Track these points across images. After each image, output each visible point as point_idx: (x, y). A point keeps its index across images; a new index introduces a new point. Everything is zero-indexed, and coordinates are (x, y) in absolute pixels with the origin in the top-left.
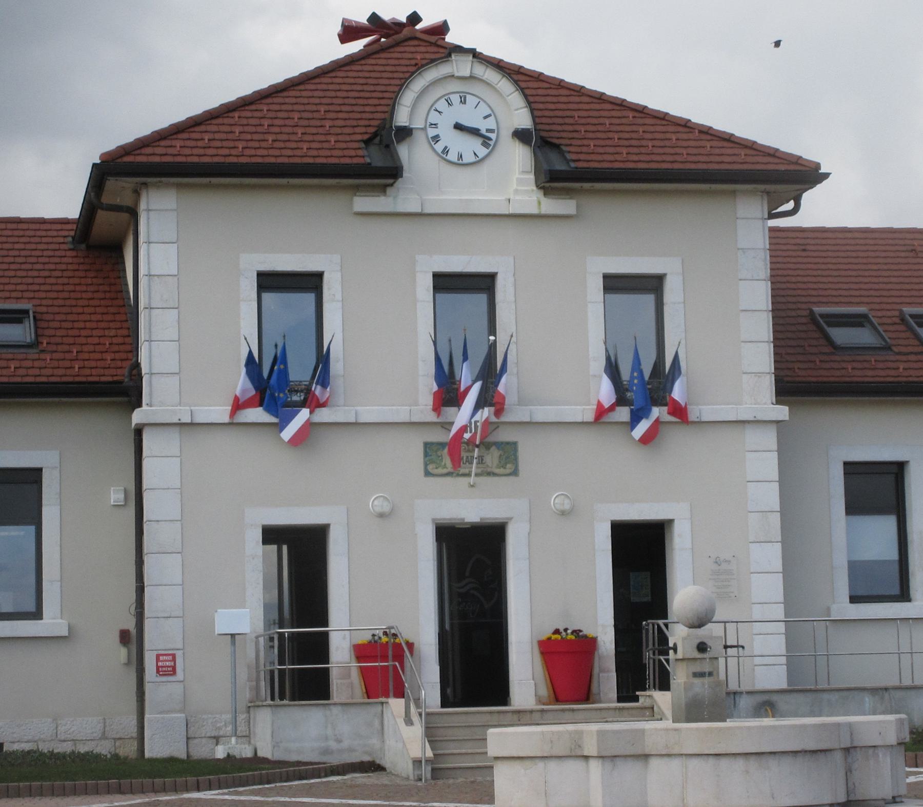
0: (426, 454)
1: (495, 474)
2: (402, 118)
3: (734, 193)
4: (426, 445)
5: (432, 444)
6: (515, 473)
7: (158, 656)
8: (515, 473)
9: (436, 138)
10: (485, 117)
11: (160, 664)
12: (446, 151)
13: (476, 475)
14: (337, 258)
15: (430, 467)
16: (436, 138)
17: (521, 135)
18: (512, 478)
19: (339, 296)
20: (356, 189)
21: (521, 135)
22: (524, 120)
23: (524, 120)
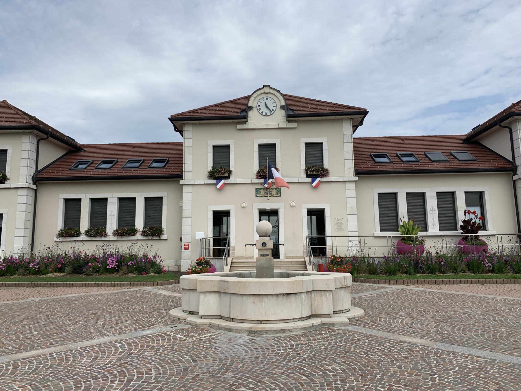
0: (256, 191)
2: (250, 104)
3: (342, 119)
4: (256, 189)
6: (280, 196)
8: (280, 196)
9: (260, 109)
14: (233, 141)
16: (260, 109)
17: (282, 107)
20: (239, 123)
21: (282, 107)
22: (283, 103)
23: (283, 103)
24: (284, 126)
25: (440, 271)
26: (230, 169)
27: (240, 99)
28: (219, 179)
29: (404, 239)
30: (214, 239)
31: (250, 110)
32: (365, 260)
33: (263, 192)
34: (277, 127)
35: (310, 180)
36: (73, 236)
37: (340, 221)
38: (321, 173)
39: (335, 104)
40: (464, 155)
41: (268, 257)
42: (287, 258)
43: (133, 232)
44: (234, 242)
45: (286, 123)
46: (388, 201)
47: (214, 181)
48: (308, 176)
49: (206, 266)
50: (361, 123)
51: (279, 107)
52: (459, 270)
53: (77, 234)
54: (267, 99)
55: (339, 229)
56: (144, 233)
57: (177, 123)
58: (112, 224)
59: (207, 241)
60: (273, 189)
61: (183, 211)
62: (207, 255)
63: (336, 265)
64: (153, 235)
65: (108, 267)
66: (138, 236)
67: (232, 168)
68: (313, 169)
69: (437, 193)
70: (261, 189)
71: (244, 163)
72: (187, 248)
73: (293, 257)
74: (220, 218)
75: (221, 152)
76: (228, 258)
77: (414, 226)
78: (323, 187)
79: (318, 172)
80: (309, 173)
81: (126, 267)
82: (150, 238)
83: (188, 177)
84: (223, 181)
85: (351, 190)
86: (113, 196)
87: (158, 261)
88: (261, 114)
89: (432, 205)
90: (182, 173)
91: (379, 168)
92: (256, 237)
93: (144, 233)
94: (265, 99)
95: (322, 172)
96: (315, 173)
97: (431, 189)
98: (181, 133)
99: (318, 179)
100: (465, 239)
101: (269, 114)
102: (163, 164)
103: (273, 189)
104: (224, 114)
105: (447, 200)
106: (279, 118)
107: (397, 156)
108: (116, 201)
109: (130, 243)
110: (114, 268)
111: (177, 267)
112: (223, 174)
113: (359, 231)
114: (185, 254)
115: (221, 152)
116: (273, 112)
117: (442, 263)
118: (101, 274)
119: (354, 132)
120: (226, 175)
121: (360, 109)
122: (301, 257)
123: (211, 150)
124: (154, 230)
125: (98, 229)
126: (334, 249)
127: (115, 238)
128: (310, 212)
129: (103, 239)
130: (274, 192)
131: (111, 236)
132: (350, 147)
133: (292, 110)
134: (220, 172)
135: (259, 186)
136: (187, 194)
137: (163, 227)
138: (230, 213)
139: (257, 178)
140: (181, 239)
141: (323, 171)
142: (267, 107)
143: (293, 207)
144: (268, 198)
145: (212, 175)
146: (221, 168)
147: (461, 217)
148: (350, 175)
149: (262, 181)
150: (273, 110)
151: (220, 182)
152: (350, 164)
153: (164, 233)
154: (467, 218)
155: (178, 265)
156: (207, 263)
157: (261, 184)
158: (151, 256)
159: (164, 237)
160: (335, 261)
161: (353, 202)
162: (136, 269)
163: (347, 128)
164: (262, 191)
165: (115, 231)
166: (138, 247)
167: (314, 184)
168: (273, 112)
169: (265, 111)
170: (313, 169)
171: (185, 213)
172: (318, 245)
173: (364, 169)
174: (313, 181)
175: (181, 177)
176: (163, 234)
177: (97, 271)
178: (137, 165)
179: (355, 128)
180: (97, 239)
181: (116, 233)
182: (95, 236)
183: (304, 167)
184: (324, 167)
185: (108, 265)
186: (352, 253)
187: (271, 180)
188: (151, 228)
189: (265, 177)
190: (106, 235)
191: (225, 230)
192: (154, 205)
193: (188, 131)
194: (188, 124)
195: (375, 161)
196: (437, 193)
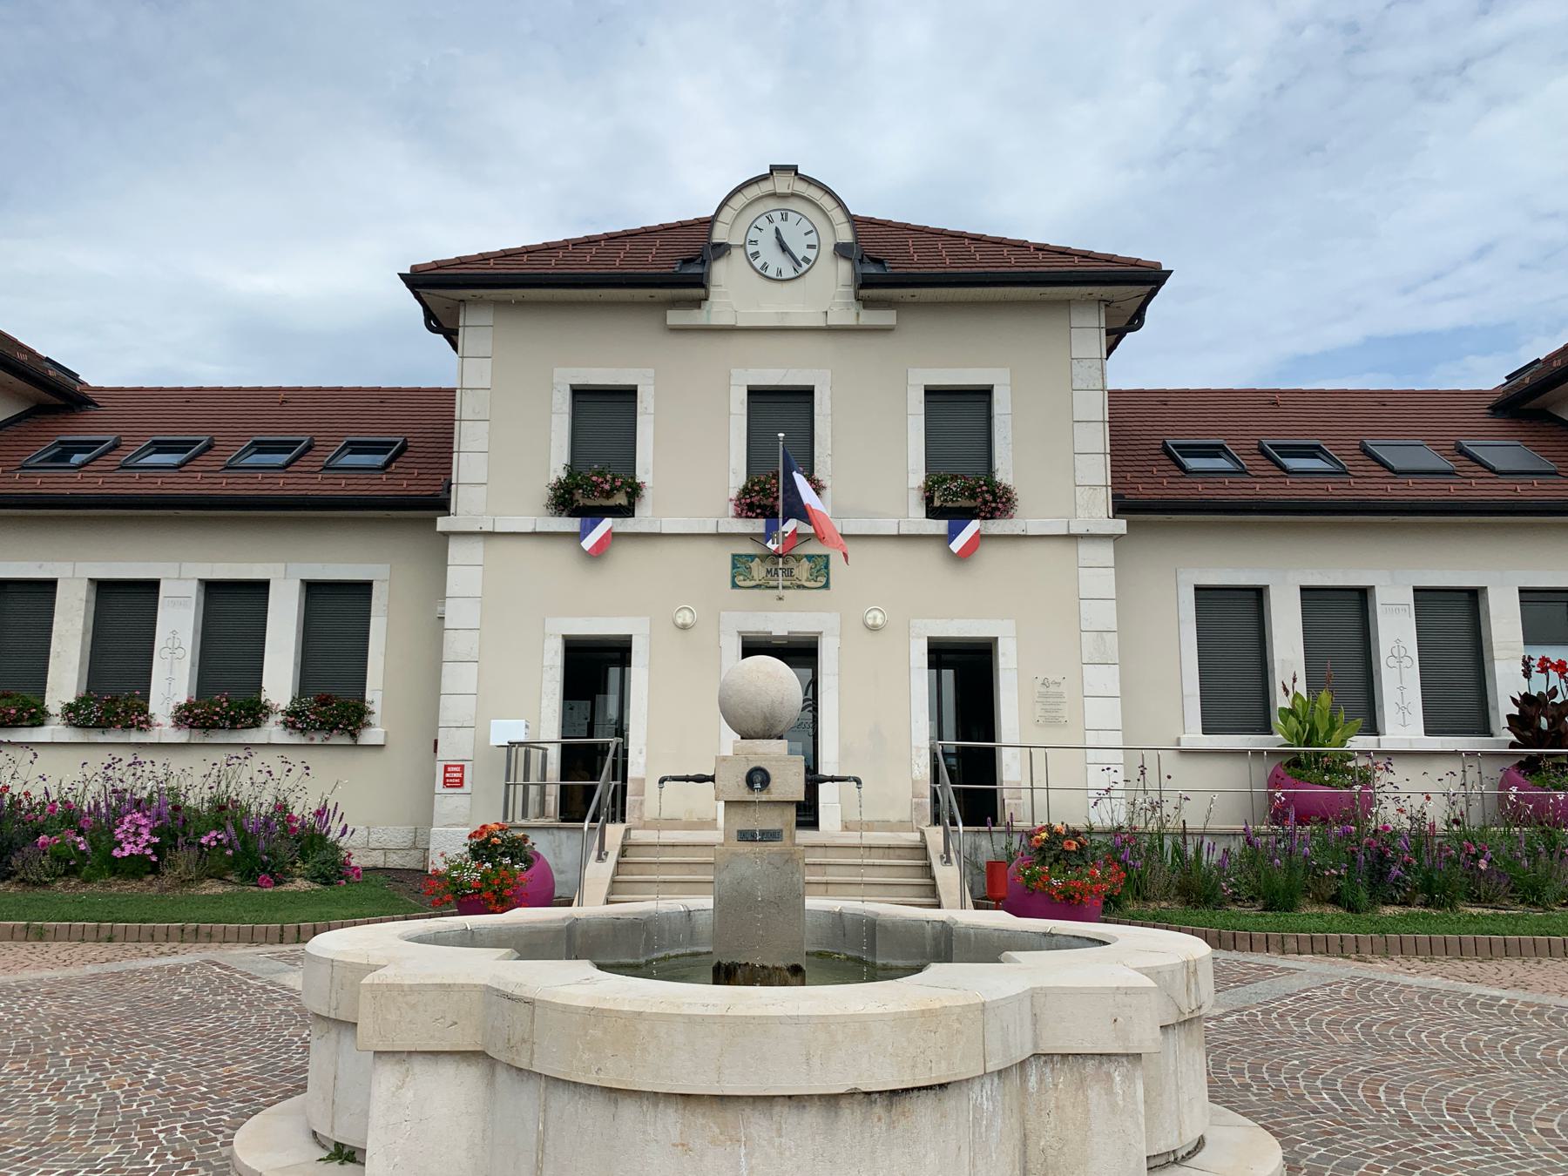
0: (734, 566)
1: (805, 587)
2: (719, 235)
3: (1067, 303)
4: (734, 556)
6: (826, 586)
7: (446, 767)
8: (826, 586)
9: (756, 255)
14: (651, 372)
15: (740, 580)
16: (756, 255)
17: (841, 251)
18: (823, 591)
20: (675, 304)
21: (841, 251)
22: (845, 235)
23: (845, 235)
24: (848, 319)
25: (1476, 900)
26: (634, 477)
27: (682, 225)
28: (593, 514)
29: (1295, 762)
30: (566, 749)
31: (717, 258)
32: (1168, 842)
33: (758, 570)
34: (822, 324)
35: (940, 526)
36: (16, 723)
37: (1053, 689)
38: (985, 502)
39: (1040, 248)
40: (1505, 452)
41: (773, 846)
43: (252, 712)
44: (642, 760)
45: (853, 311)
46: (1231, 617)
47: (572, 524)
48: (933, 513)
49: (507, 861)
50: (1136, 320)
51: (827, 248)
52: (1549, 893)
53: (32, 716)
54: (784, 218)
56: (295, 719)
57: (436, 296)
58: (172, 678)
59: (536, 755)
60: (798, 559)
61: (447, 634)
62: (533, 808)
63: (1057, 868)
64: (329, 726)
65: (116, 852)
66: (272, 731)
67: (642, 475)
68: (953, 486)
69: (1416, 590)
70: (752, 557)
71: (691, 460)
72: (454, 780)
73: (870, 826)
74: (593, 668)
75: (604, 412)
76: (609, 827)
77: (1334, 710)
78: (987, 553)
79: (973, 496)
80: (937, 503)
81: (193, 853)
82: (317, 741)
83: (470, 505)
84: (607, 524)
85: (1096, 572)
86: (180, 571)
87: (335, 828)
88: (762, 273)
89: (1397, 635)
90: (449, 491)
92: (729, 740)
93: (295, 719)
94: (776, 216)
95: (988, 497)
96: (963, 503)
97: (1394, 577)
98: (452, 337)
99: (974, 526)
100: (1530, 767)
101: (793, 275)
102: (380, 459)
103: (798, 559)
105: (1452, 616)
106: (828, 291)
107: (1263, 451)
108: (192, 591)
109: (220, 756)
110: (142, 858)
111: (417, 854)
112: (609, 494)
113: (1125, 729)
114: (448, 803)
115: (604, 412)
116: (805, 266)
117: (1483, 865)
118: (87, 881)
119: (1109, 352)
120: (621, 499)
122: (901, 826)
124: (332, 709)
125: (114, 701)
126: (1040, 795)
127: (182, 736)
128: (941, 654)
129: (135, 737)
130: (803, 571)
131: (164, 728)
132: (1095, 408)
133: (878, 262)
134: (597, 487)
135: (747, 548)
136: (466, 568)
137: (368, 697)
138: (629, 650)
139: (739, 516)
142: (784, 248)
143: (874, 629)
144: (781, 592)
145: (565, 499)
146: (599, 474)
147: (1508, 682)
148: (1096, 512)
149: (759, 526)
150: (806, 260)
151: (595, 525)
152: (1096, 471)
153: (373, 719)
154: (1538, 685)
155: (421, 845)
156: (517, 849)
157: (752, 537)
158: (303, 808)
159: (370, 736)
160: (1056, 850)
161: (1104, 614)
162: (233, 864)
163: (1087, 333)
164: (755, 564)
165: (180, 708)
166: (268, 773)
167: (956, 546)
168: (805, 266)
169: (777, 262)
170: (953, 486)
171: (455, 644)
172: (969, 777)
173: (1144, 491)
174: (953, 534)
176: (369, 725)
177: (69, 867)
178: (283, 459)
179: (1115, 336)
180: (111, 737)
181: (186, 717)
182: (103, 725)
183: (918, 477)
184: (998, 478)
185: (119, 843)
186: (1108, 815)
187: (791, 525)
188: (324, 701)
189: (769, 514)
190: (146, 724)
191: (613, 712)
192: (337, 610)
193: (478, 328)
194: (479, 302)
195: (1178, 467)
196: (1416, 590)
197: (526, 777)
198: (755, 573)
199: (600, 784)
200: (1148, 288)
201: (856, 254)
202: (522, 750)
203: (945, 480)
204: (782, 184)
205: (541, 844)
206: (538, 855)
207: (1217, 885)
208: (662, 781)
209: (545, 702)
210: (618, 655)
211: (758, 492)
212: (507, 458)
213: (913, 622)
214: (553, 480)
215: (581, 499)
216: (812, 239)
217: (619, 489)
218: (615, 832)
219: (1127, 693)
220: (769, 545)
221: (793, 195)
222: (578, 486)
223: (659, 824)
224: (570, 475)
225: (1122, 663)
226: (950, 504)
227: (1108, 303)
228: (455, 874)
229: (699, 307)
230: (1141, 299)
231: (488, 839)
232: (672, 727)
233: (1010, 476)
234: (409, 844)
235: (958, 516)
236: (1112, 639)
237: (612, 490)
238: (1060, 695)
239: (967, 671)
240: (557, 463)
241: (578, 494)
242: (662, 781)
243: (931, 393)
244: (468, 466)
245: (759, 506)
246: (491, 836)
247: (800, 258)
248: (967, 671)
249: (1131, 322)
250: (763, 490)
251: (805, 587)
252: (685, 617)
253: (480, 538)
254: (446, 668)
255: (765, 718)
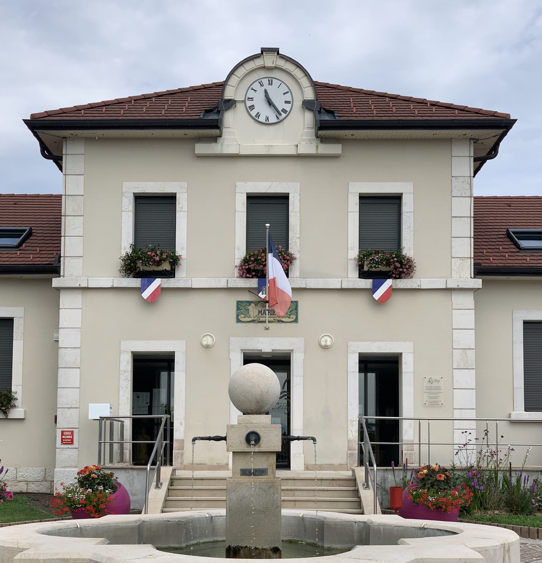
0: (238, 309)
1: (282, 322)
2: (229, 94)
3: (450, 141)
4: (239, 303)
5: (242, 302)
7: (62, 432)
8: (296, 321)
9: (252, 107)
10: (284, 94)
11: (64, 437)
12: (258, 115)
13: (269, 322)
14: (185, 184)
15: (242, 318)
16: (252, 107)
17: (307, 105)
19: (185, 209)
21: (307, 105)
22: (310, 95)
23: (310, 95)
24: (312, 150)
26: (174, 252)
30: (135, 422)
31: (228, 109)
33: (253, 311)
34: (293, 152)
35: (367, 283)
37: (435, 384)
38: (396, 268)
42: (307, 468)
44: (182, 428)
45: (314, 144)
47: (136, 282)
48: (363, 275)
51: (298, 103)
54: (270, 84)
55: (434, 403)
61: (61, 351)
67: (181, 249)
68: (376, 258)
70: (250, 303)
71: (210, 239)
72: (68, 439)
74: (151, 372)
75: (156, 209)
78: (397, 300)
79: (388, 264)
80: (366, 268)
84: (157, 282)
85: (463, 313)
88: (256, 119)
90: (59, 261)
91: (529, 261)
92: (235, 415)
94: (265, 82)
95: (398, 265)
98: (58, 161)
99: (389, 282)
101: (274, 120)
104: (163, 114)
106: (297, 132)
112: (159, 263)
113: (477, 409)
114: (65, 454)
115: (156, 209)
119: (475, 172)
120: (166, 266)
121: (494, 114)
123: (129, 205)
128: (367, 363)
132: (465, 208)
134: (151, 259)
135: (246, 297)
136: (72, 312)
137: (14, 389)
138: (173, 361)
139: (241, 276)
140: (56, 417)
141: (401, 263)
142: (270, 103)
143: (325, 348)
144: (267, 325)
148: (463, 274)
150: (284, 111)
152: (464, 248)
153: (18, 403)
155: (49, 479)
157: (250, 290)
159: (16, 413)
161: (466, 339)
163: (462, 160)
164: (251, 307)
167: (377, 295)
168: (284, 115)
169: (265, 112)
170: (376, 258)
171: (66, 357)
175: (55, 270)
176: (15, 406)
179: (479, 162)
183: (354, 252)
193: (75, 155)
194: (75, 139)
197: (111, 438)
198: (251, 313)
199: (157, 443)
200: (501, 131)
201: (316, 107)
202: (108, 422)
203: (371, 254)
204: (269, 60)
205: (121, 478)
206: (119, 484)
207: (529, 501)
208: (194, 440)
209: (121, 393)
210: (166, 364)
211: (253, 262)
212: (95, 240)
213: (350, 343)
214: (124, 254)
215: (141, 266)
216: (288, 97)
217: (165, 260)
218: (166, 471)
219: (480, 388)
220: (260, 295)
221: (276, 68)
222: (139, 258)
223: (193, 467)
224: (134, 251)
225: (477, 369)
226: (374, 269)
227: (475, 141)
228: (70, 495)
229: (216, 141)
230: (497, 138)
231: (89, 475)
232: (197, 407)
233: (412, 252)
234: (41, 478)
235: (378, 277)
236: (471, 354)
237: (160, 261)
238: (438, 388)
239: (383, 374)
240: (126, 242)
241: (139, 264)
242: (194, 440)
243: (363, 198)
244: (71, 245)
245: (254, 270)
246: (91, 473)
247: (280, 110)
248: (383, 374)
249: (490, 153)
250: (256, 260)
251: (282, 322)
252: (208, 341)
253: (80, 292)
254: (61, 372)
255: (258, 402)
